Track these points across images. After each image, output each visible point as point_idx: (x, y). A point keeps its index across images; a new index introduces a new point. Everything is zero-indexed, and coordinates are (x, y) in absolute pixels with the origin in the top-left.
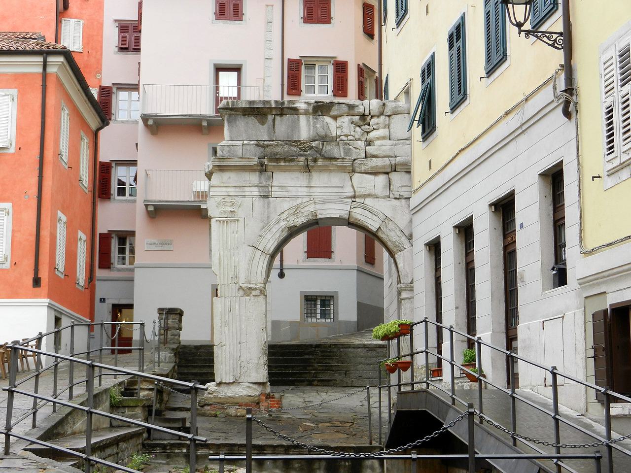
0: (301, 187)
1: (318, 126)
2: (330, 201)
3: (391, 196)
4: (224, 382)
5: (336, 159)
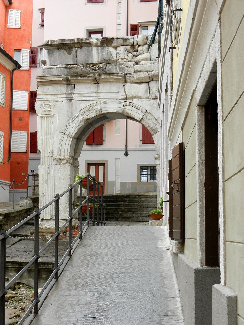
0: (92, 93)
1: (104, 53)
2: (110, 102)
3: (150, 97)
5: (113, 74)
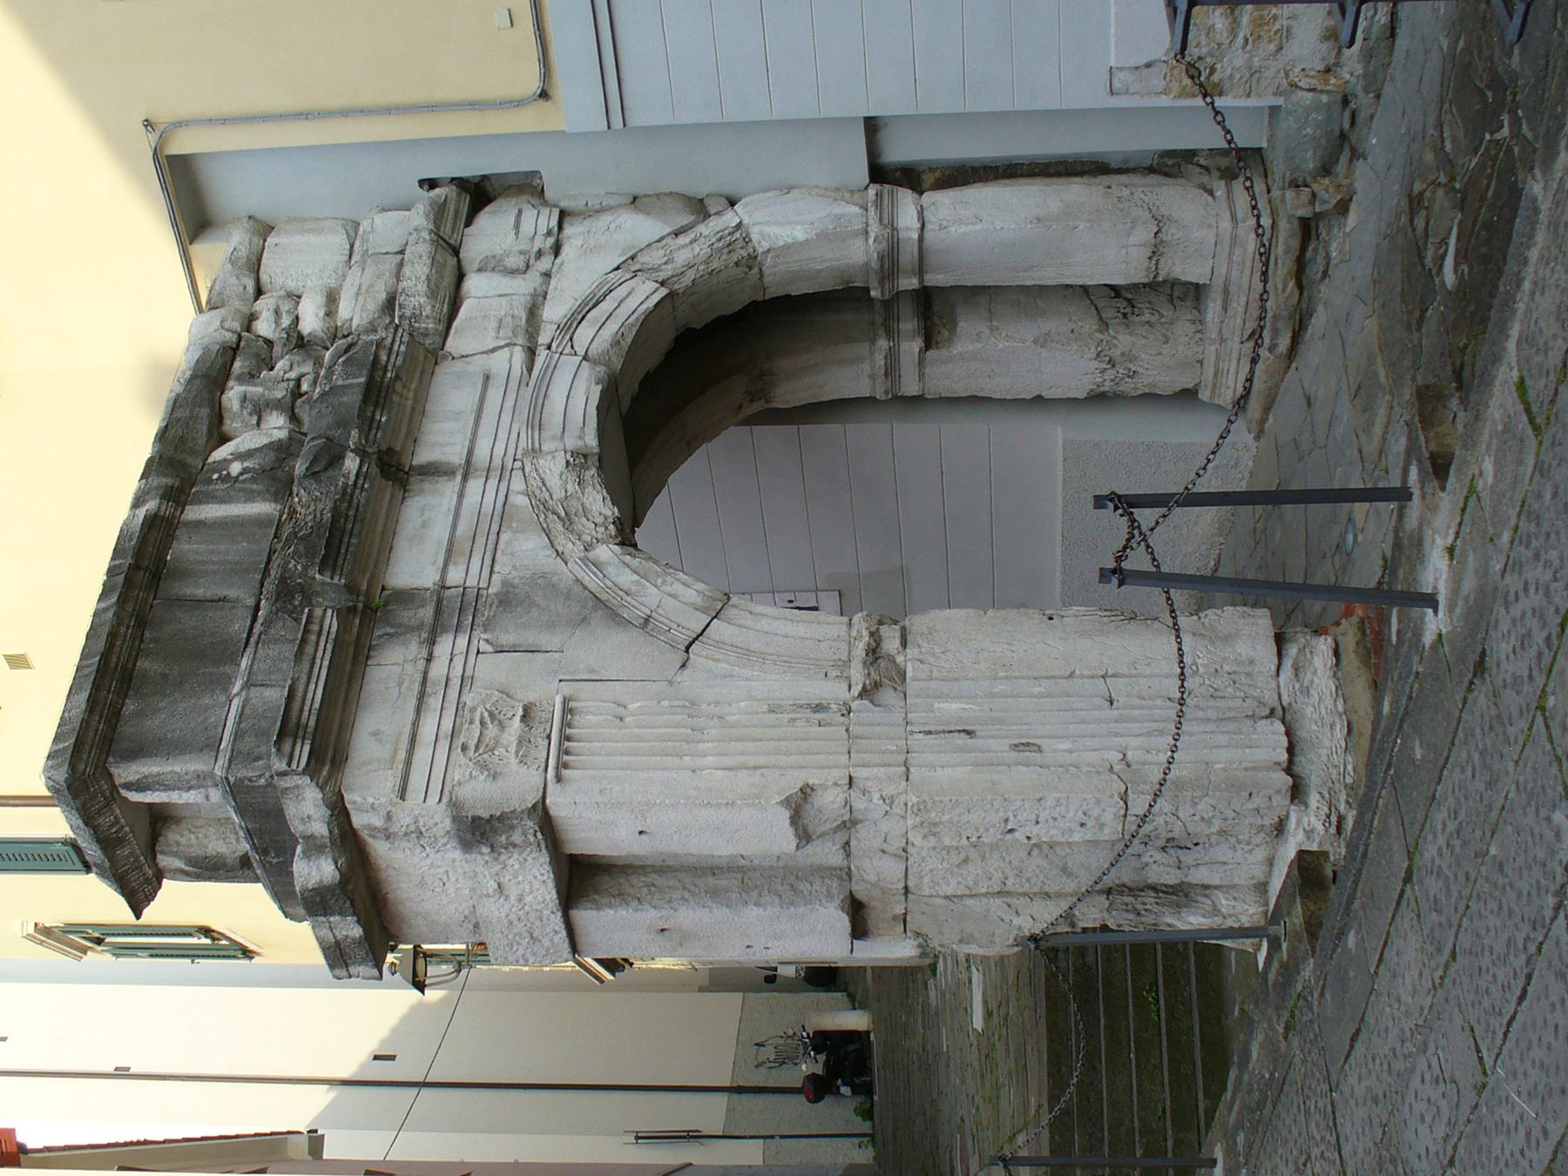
4: (1285, 756)
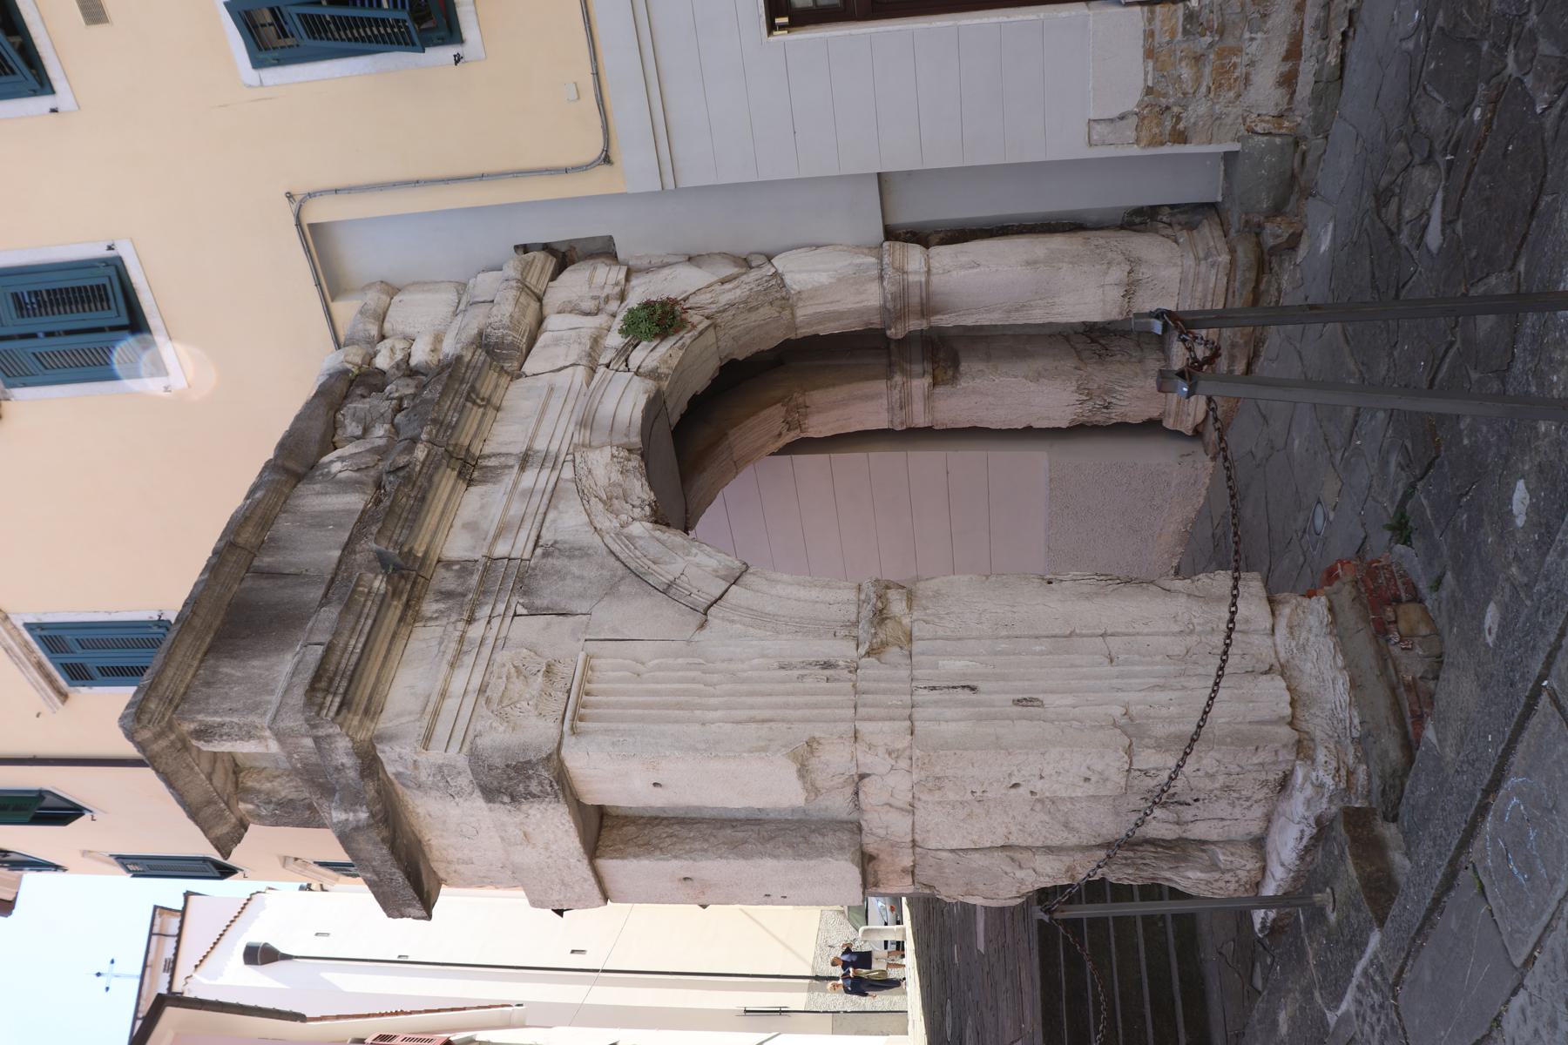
4: (1288, 711)
